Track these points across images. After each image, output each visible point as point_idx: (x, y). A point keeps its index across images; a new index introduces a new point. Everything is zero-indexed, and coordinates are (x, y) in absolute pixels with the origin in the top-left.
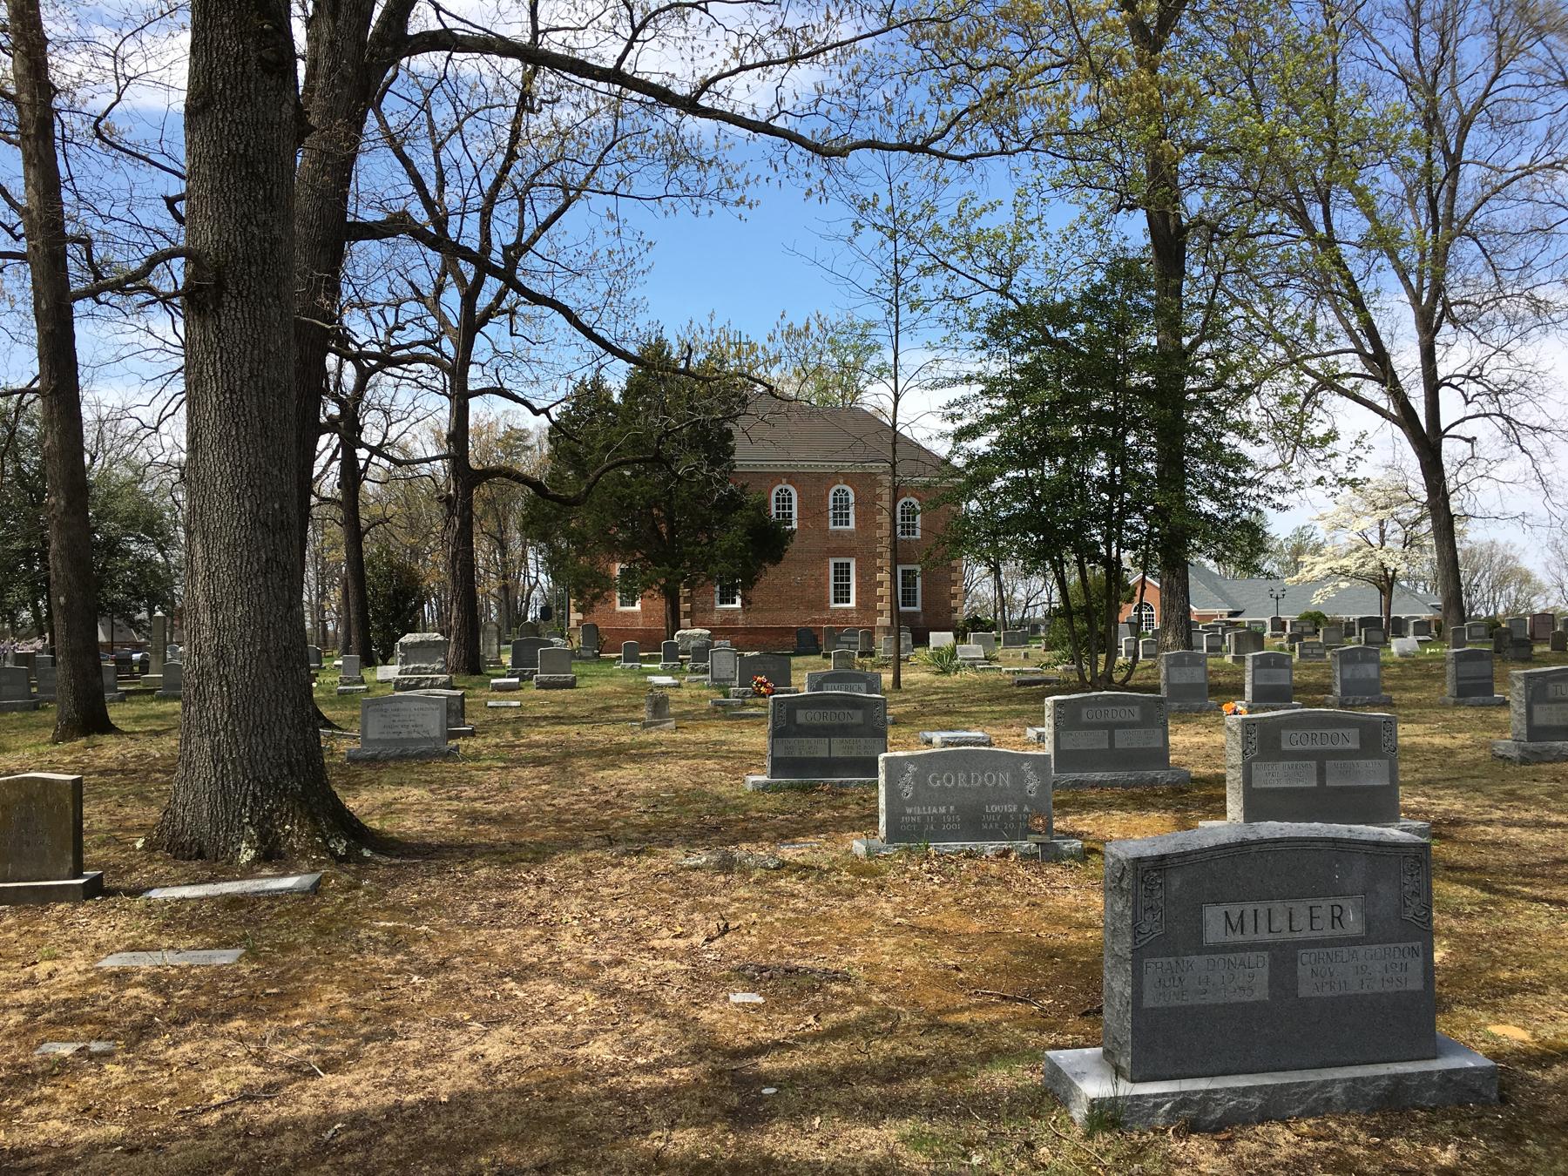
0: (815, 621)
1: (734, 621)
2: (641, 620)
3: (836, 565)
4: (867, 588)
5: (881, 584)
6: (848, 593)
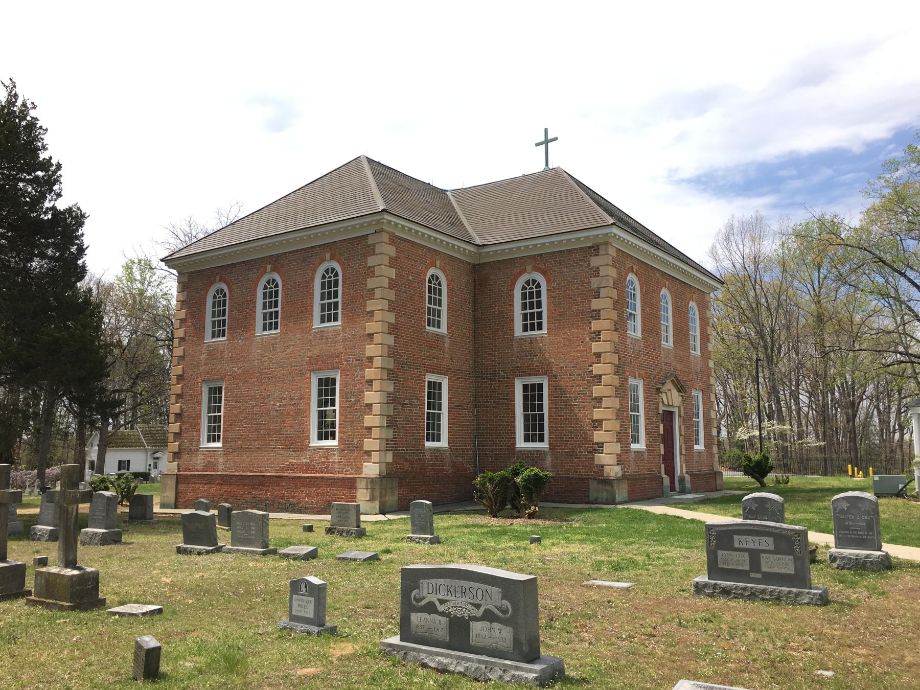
0: (291, 467)
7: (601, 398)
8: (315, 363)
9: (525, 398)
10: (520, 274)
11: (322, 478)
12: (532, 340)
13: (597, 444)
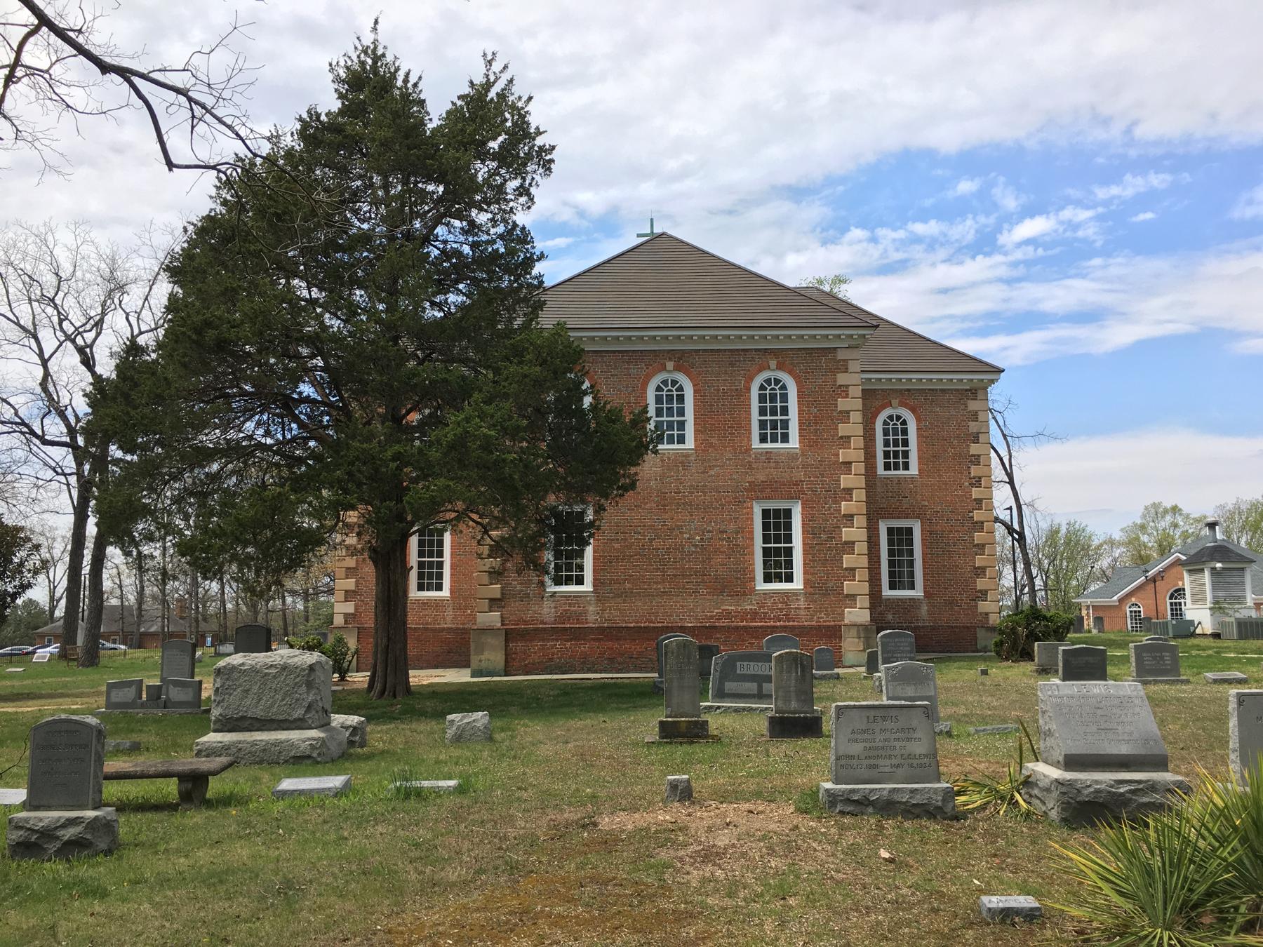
0: (727, 615)
2: (449, 614)
3: (766, 513)
4: (825, 548)
5: (850, 546)
6: (789, 564)
7: (983, 545)
8: (758, 491)
9: (890, 542)
10: (883, 407)
12: (900, 480)
13: (981, 591)
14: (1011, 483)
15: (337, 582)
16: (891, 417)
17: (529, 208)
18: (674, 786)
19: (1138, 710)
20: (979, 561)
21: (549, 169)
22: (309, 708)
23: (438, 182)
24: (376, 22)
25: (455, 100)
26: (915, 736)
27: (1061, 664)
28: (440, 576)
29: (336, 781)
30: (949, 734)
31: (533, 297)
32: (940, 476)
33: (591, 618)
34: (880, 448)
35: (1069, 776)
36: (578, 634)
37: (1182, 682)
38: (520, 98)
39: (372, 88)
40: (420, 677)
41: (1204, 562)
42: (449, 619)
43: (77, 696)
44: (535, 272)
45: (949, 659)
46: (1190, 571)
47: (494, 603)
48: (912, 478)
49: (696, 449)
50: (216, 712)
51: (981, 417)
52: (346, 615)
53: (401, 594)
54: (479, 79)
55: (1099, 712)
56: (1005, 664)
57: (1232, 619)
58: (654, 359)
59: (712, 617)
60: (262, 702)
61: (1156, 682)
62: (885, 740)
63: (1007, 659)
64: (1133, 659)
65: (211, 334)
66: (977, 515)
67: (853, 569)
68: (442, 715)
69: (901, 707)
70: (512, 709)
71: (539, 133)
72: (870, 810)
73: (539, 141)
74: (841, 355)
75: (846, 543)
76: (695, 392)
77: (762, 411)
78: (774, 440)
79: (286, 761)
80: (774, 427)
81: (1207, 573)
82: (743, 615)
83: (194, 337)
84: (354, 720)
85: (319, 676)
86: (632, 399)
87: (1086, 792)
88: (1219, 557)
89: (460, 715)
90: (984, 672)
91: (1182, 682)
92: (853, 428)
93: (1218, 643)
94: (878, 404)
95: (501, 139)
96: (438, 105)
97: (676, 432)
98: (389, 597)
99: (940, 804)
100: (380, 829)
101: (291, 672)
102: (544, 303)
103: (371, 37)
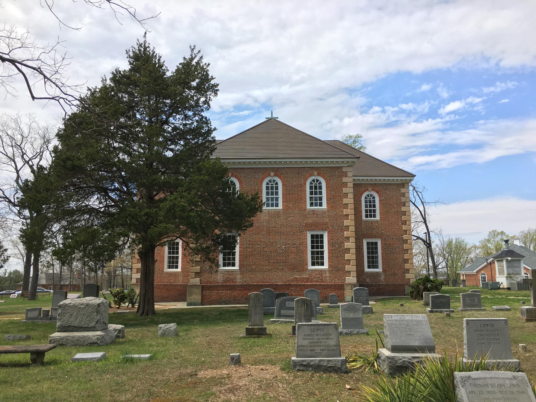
0: (296, 279)
1: (233, 280)
2: (181, 279)
3: (312, 236)
4: (337, 251)
5: (348, 250)
6: (322, 258)
7: (408, 250)
9: (368, 248)
10: (365, 191)
11: (321, 285)
12: (372, 222)
13: (407, 269)
14: (425, 222)
15: (127, 265)
16: (368, 196)
17: (208, 109)
18: (232, 358)
19: (424, 326)
20: (406, 256)
21: (217, 93)
22: (97, 322)
23: (168, 99)
24: (145, 33)
25: (178, 65)
26: (331, 337)
27: (431, 302)
28: (177, 262)
29: (99, 355)
30: (367, 334)
31: (211, 145)
32: (389, 220)
33: (238, 281)
34: (363, 208)
35: (393, 355)
36: (232, 288)
37: (482, 310)
38: (206, 64)
39: (144, 60)
40: (159, 306)
41: (503, 257)
42: (181, 281)
43: (17, 313)
44: (212, 135)
45: (393, 299)
46: (498, 261)
47: (197, 274)
48: (377, 221)
49: (283, 209)
50: (58, 324)
51: (406, 195)
52: (137, 279)
53: (151, 271)
54: (188, 57)
55: (408, 327)
56: (414, 301)
57: (515, 282)
58: (265, 171)
59: (289, 280)
60: (78, 319)
61: (471, 310)
62: (318, 339)
63: (415, 299)
64: (461, 300)
65: (69, 163)
66: (405, 237)
67: (350, 260)
68: (158, 323)
69: (325, 325)
70: (195, 321)
71: (212, 78)
72: (311, 369)
73: (212, 82)
74: (344, 170)
75: (346, 249)
76: (283, 185)
77: (311, 193)
78: (316, 205)
79: (87, 345)
80: (316, 200)
81: (504, 262)
82: (303, 280)
83: (62, 164)
84: (120, 327)
85: (102, 308)
86: (256, 188)
87: (399, 362)
88: (510, 255)
89: (164, 325)
90: (402, 305)
91: (482, 310)
92: (349, 200)
93: (510, 292)
94: (362, 189)
95: (197, 80)
96: (171, 66)
97: (274, 202)
98: (146, 272)
99: (340, 366)
100: (108, 376)
101: (90, 307)
102: (216, 148)
103: (143, 40)
